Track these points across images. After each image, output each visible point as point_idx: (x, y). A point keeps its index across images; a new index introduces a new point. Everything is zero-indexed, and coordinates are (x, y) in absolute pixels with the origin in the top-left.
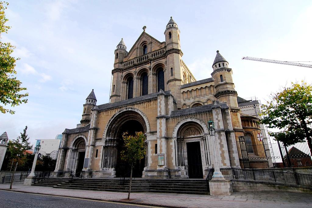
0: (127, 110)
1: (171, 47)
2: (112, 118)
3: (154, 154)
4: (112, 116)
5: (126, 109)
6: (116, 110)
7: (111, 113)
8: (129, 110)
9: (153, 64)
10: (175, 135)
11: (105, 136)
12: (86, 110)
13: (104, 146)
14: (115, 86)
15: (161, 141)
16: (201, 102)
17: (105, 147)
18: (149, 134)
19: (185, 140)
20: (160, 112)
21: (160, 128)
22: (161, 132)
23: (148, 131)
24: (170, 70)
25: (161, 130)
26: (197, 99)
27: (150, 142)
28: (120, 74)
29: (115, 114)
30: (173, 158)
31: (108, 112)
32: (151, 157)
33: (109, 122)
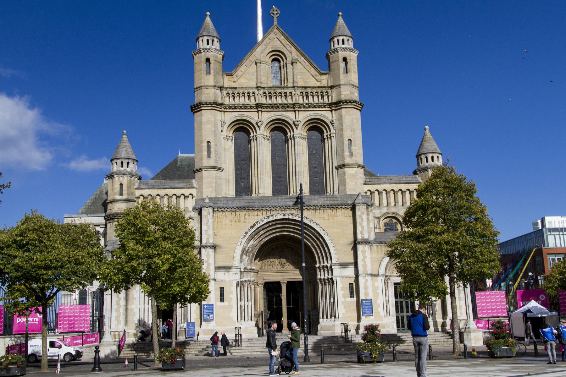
0: (286, 217)
1: (348, 93)
2: (252, 227)
3: (349, 299)
4: (252, 225)
5: (284, 215)
6: (260, 213)
7: (247, 217)
8: (291, 217)
9: (303, 116)
10: (382, 271)
11: (237, 263)
12: (125, 187)
13: (238, 283)
14: (212, 144)
15: (366, 281)
16: (398, 214)
17: (240, 284)
18: (337, 267)
19: (391, 278)
20: (362, 233)
21: (363, 260)
22: (365, 266)
23: (334, 261)
24: (346, 142)
25: (365, 262)
26: (393, 210)
27: (339, 280)
28: (219, 116)
29: (258, 222)
30: (379, 304)
31: (238, 213)
32: (343, 303)
33: (245, 236)
